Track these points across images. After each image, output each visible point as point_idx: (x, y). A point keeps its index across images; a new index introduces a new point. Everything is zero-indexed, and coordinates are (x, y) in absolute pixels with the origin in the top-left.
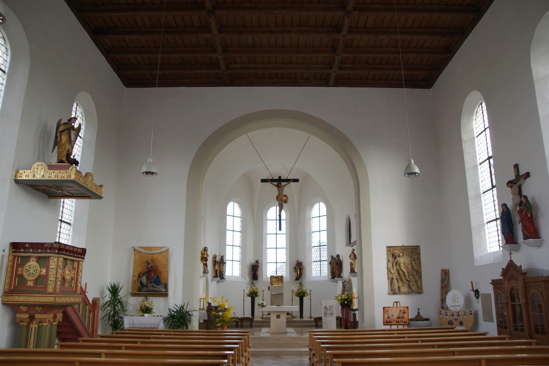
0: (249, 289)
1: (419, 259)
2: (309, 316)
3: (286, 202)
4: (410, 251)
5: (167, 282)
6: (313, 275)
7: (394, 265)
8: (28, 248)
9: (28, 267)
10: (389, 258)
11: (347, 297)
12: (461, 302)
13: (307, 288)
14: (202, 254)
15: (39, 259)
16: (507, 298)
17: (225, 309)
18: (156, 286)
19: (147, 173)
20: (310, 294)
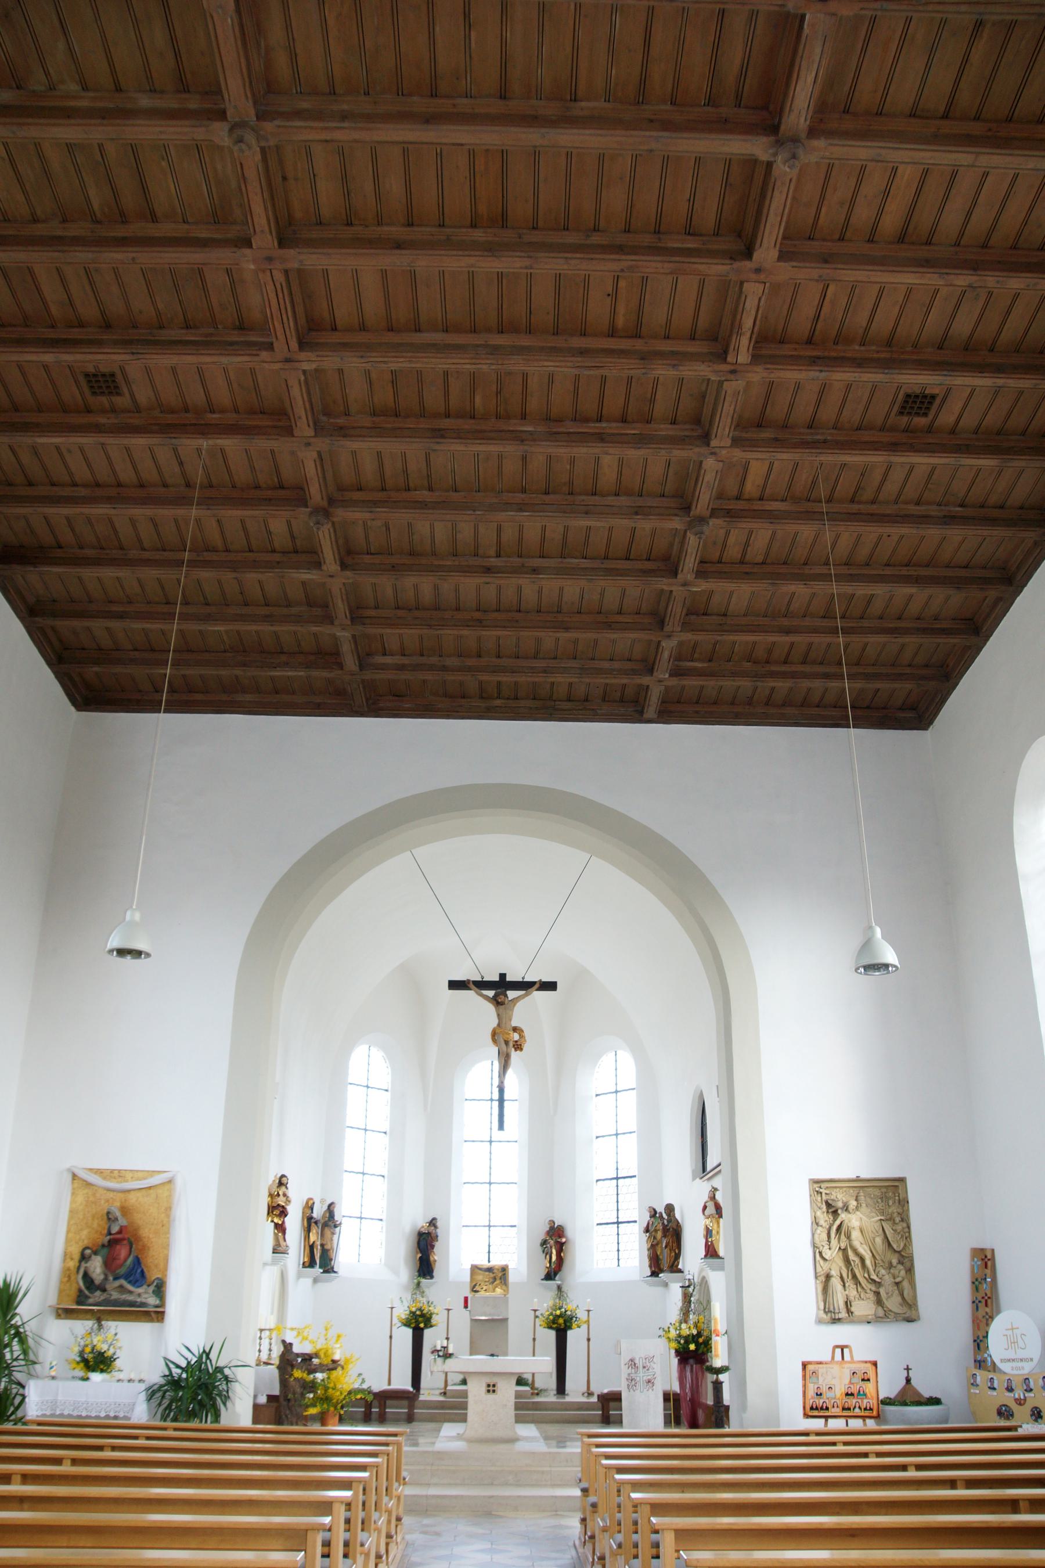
0: (406, 1304)
1: (905, 1218)
2: (585, 1389)
3: (518, 1047)
4: (877, 1192)
5: (166, 1276)
10: (819, 1213)
11: (695, 1332)
13: (577, 1303)
14: (271, 1195)
17: (334, 1362)
19: (122, 952)
20: (588, 1322)
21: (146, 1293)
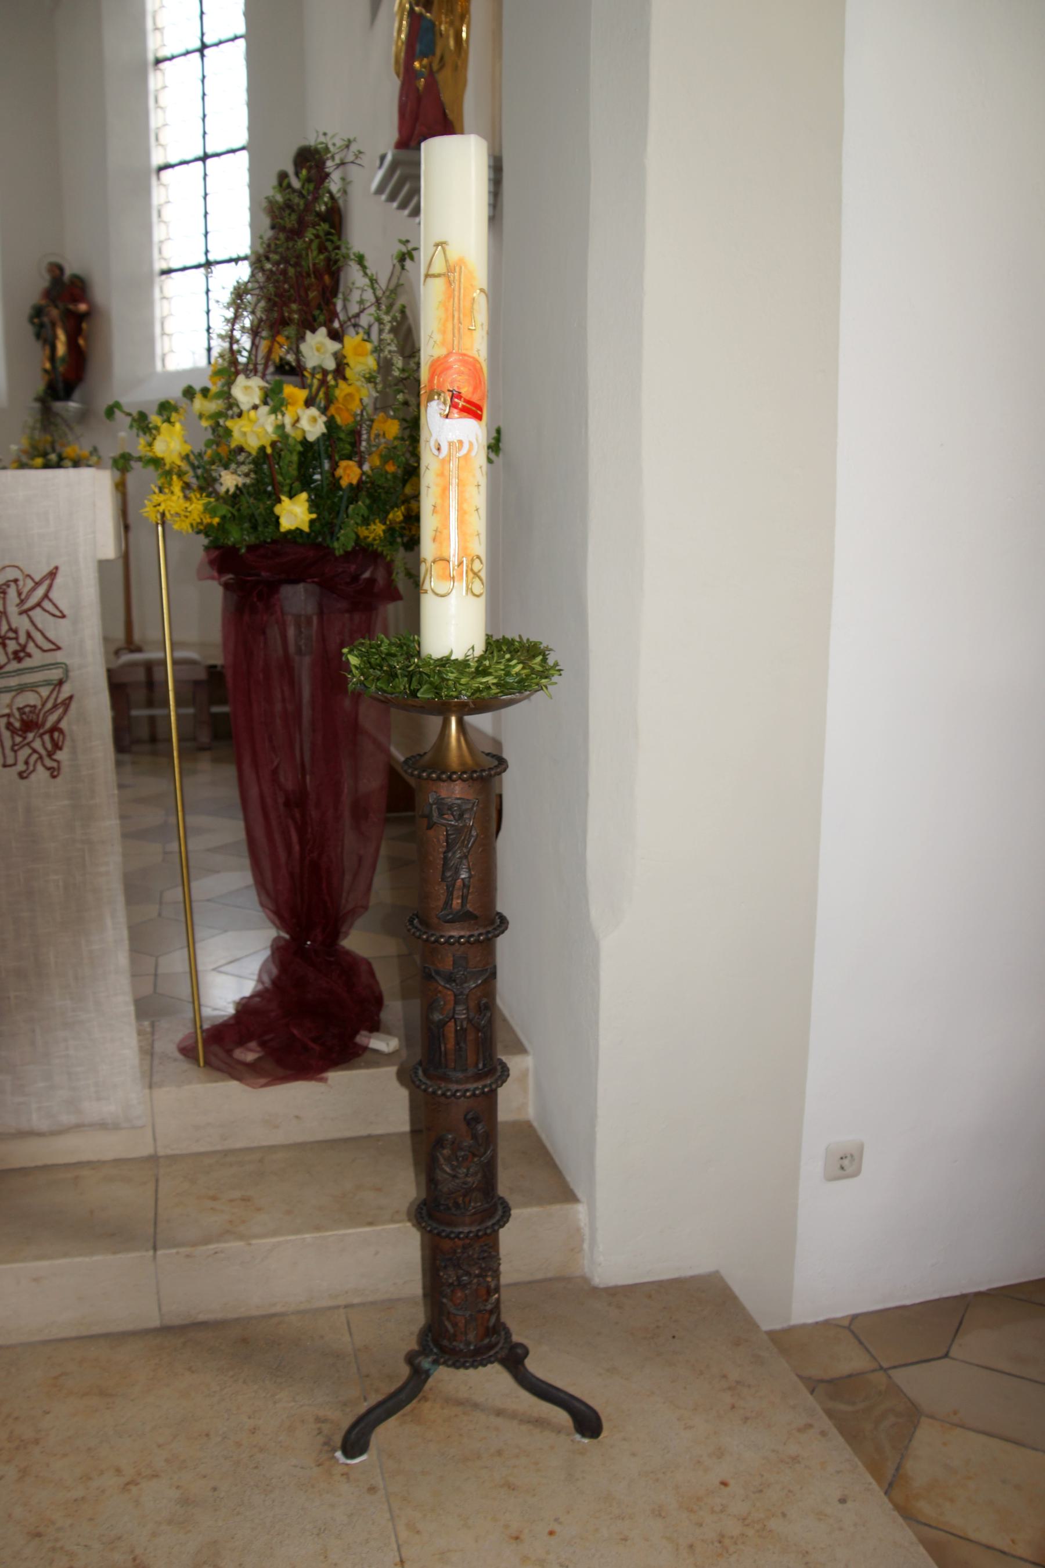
6: (159, 367)
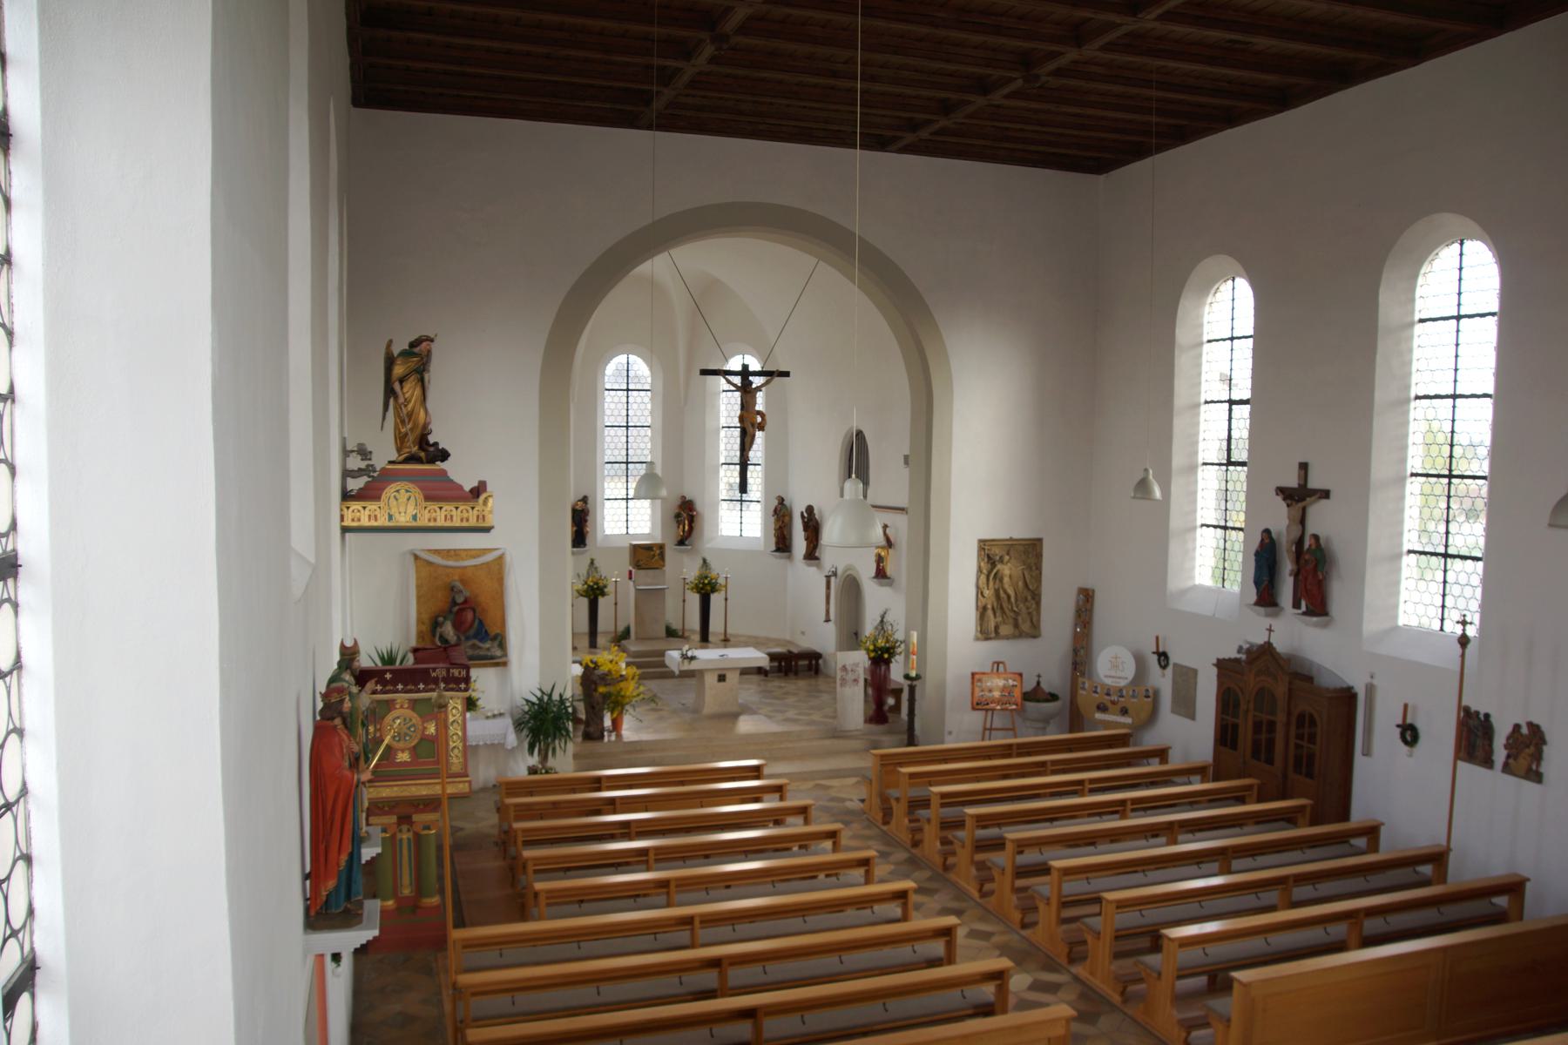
0: (582, 578)
1: (1039, 568)
4: (1021, 548)
7: (991, 578)
8: (394, 682)
9: (409, 728)
10: (982, 564)
12: (1129, 671)
13: (719, 570)
15: (414, 704)
16: (1249, 702)
17: (621, 676)
18: (481, 645)
20: (726, 586)
21: (492, 647)
